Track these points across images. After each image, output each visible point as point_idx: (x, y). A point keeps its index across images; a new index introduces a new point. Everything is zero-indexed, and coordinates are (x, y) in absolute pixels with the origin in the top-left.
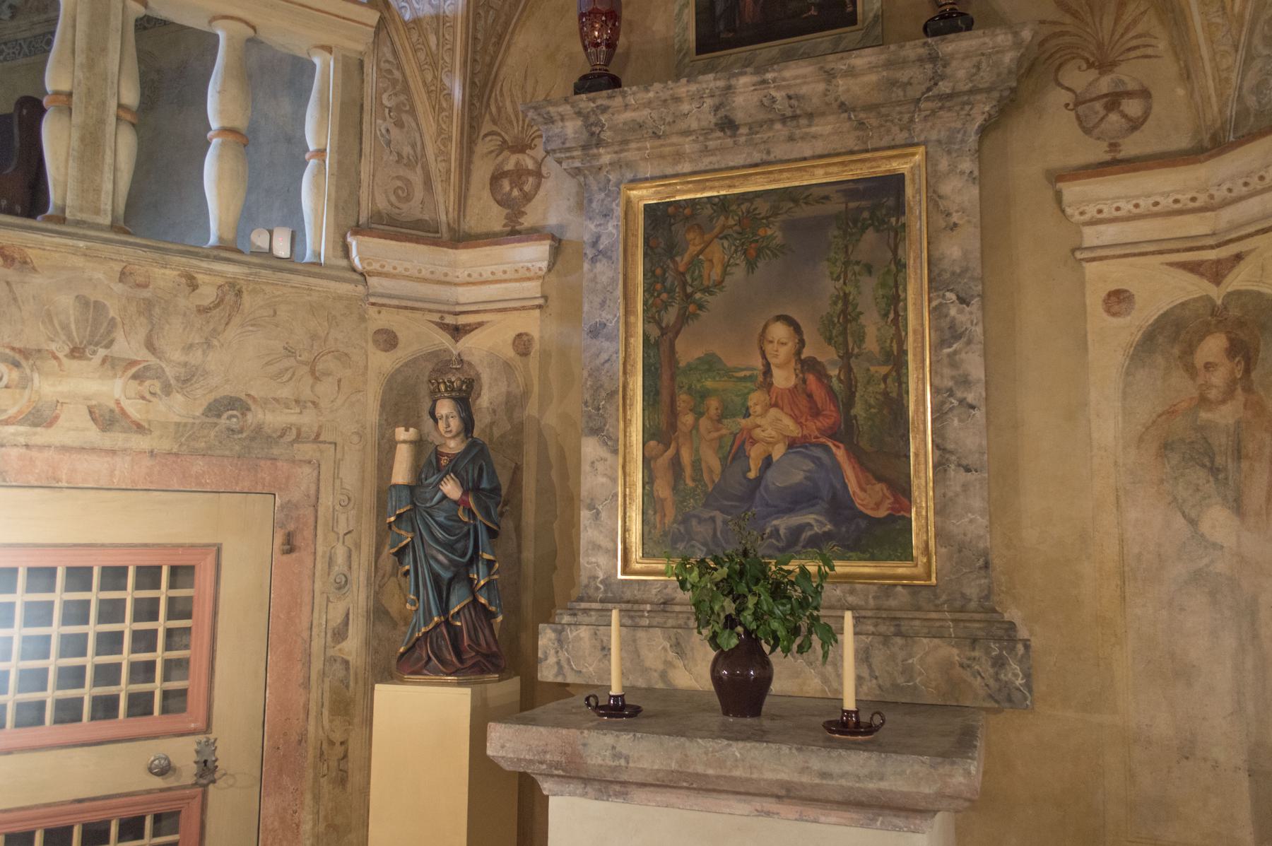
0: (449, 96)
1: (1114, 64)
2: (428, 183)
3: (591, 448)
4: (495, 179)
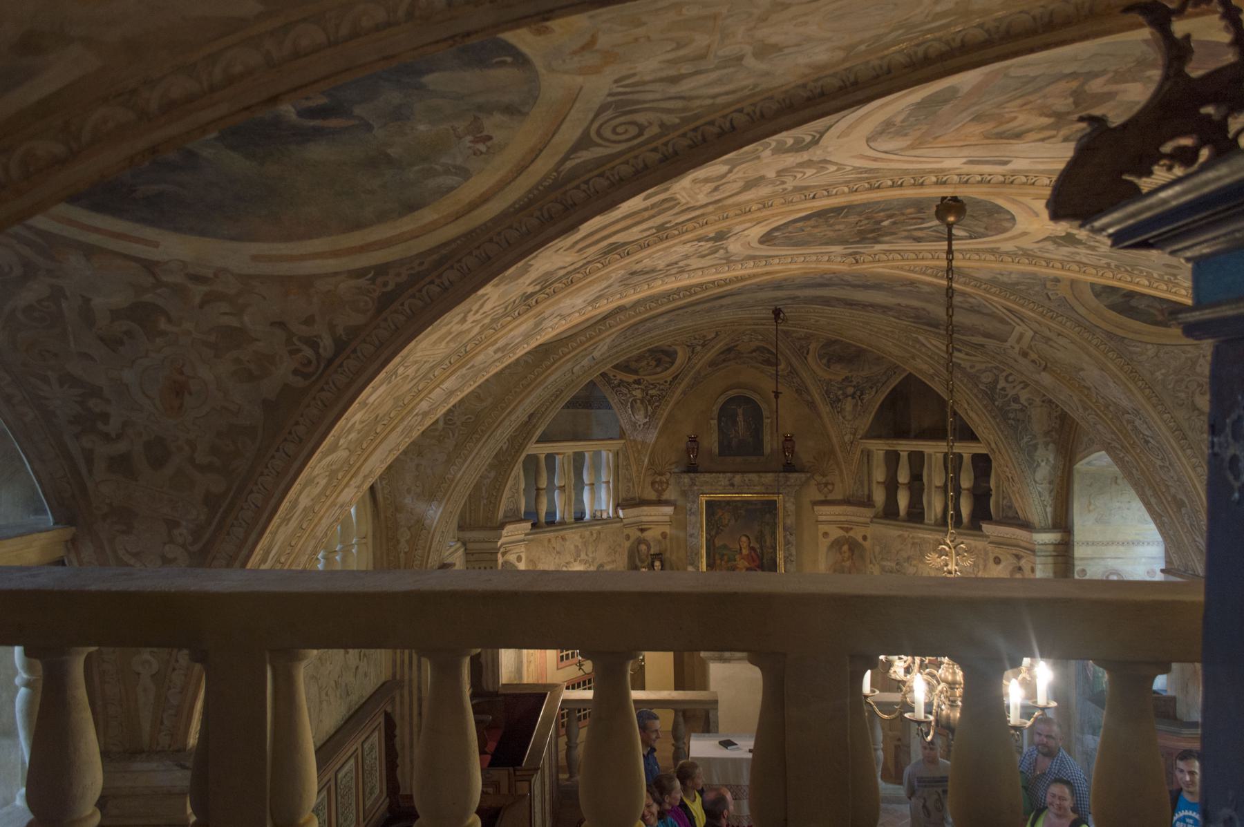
0: (643, 462)
1: (826, 476)
2: (634, 487)
4: (653, 483)
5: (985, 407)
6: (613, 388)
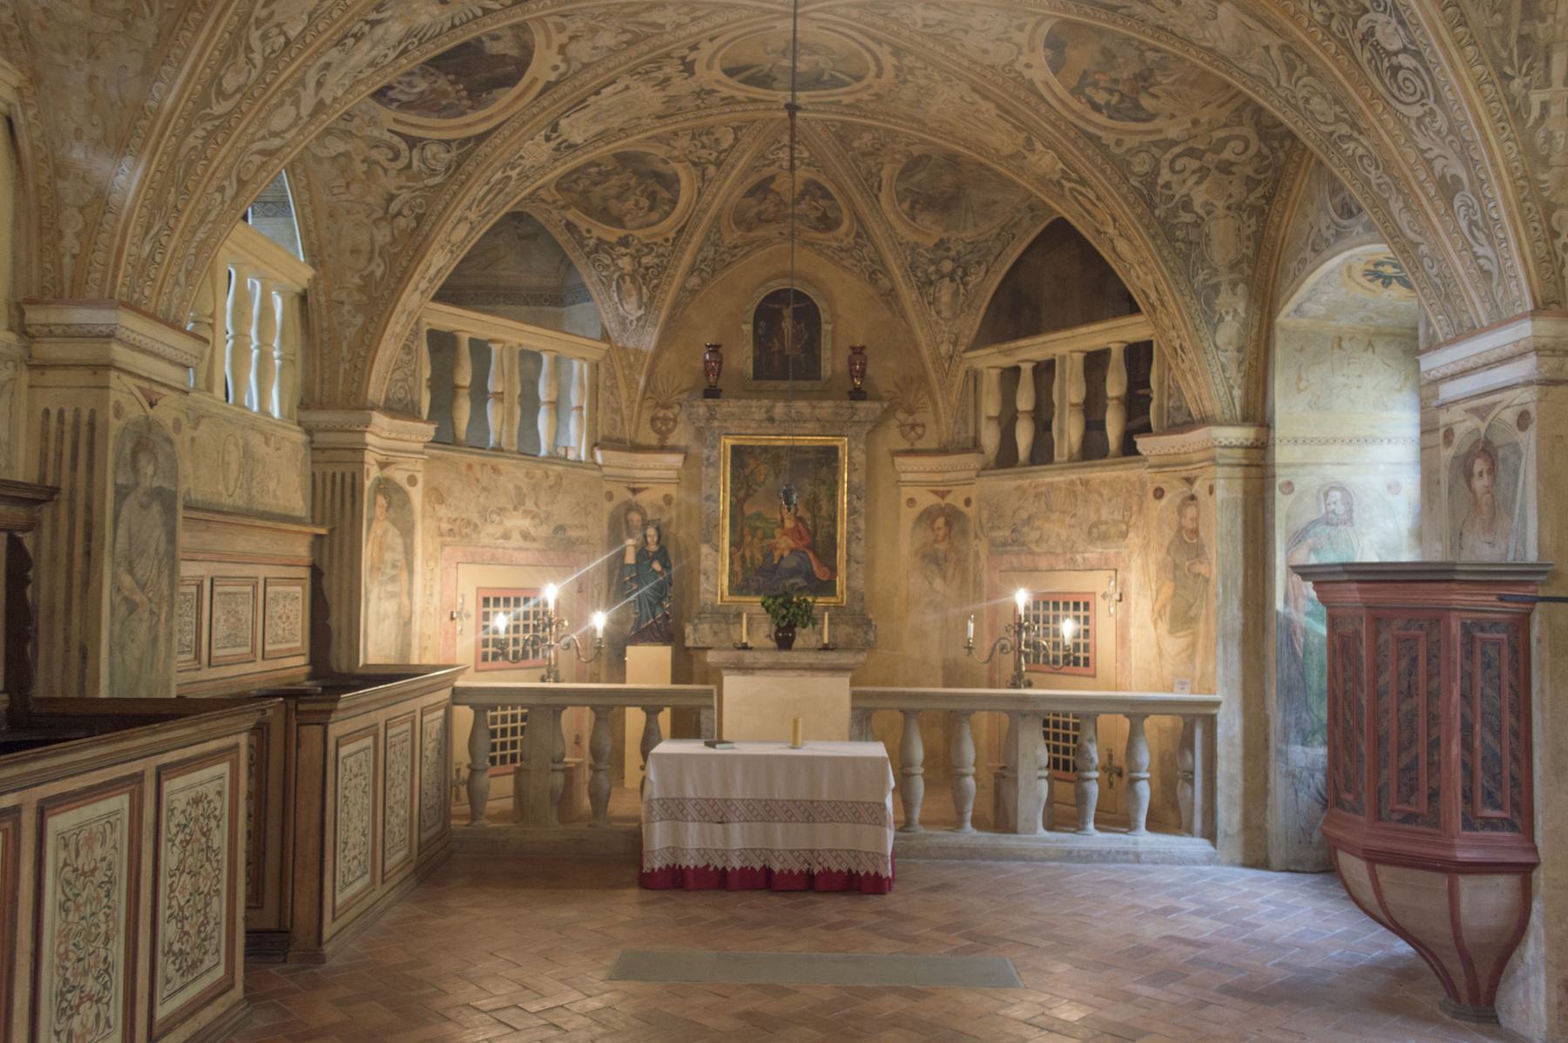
0: (638, 383)
3: (705, 549)
4: (653, 420)
5: (1140, 218)
6: (588, 255)
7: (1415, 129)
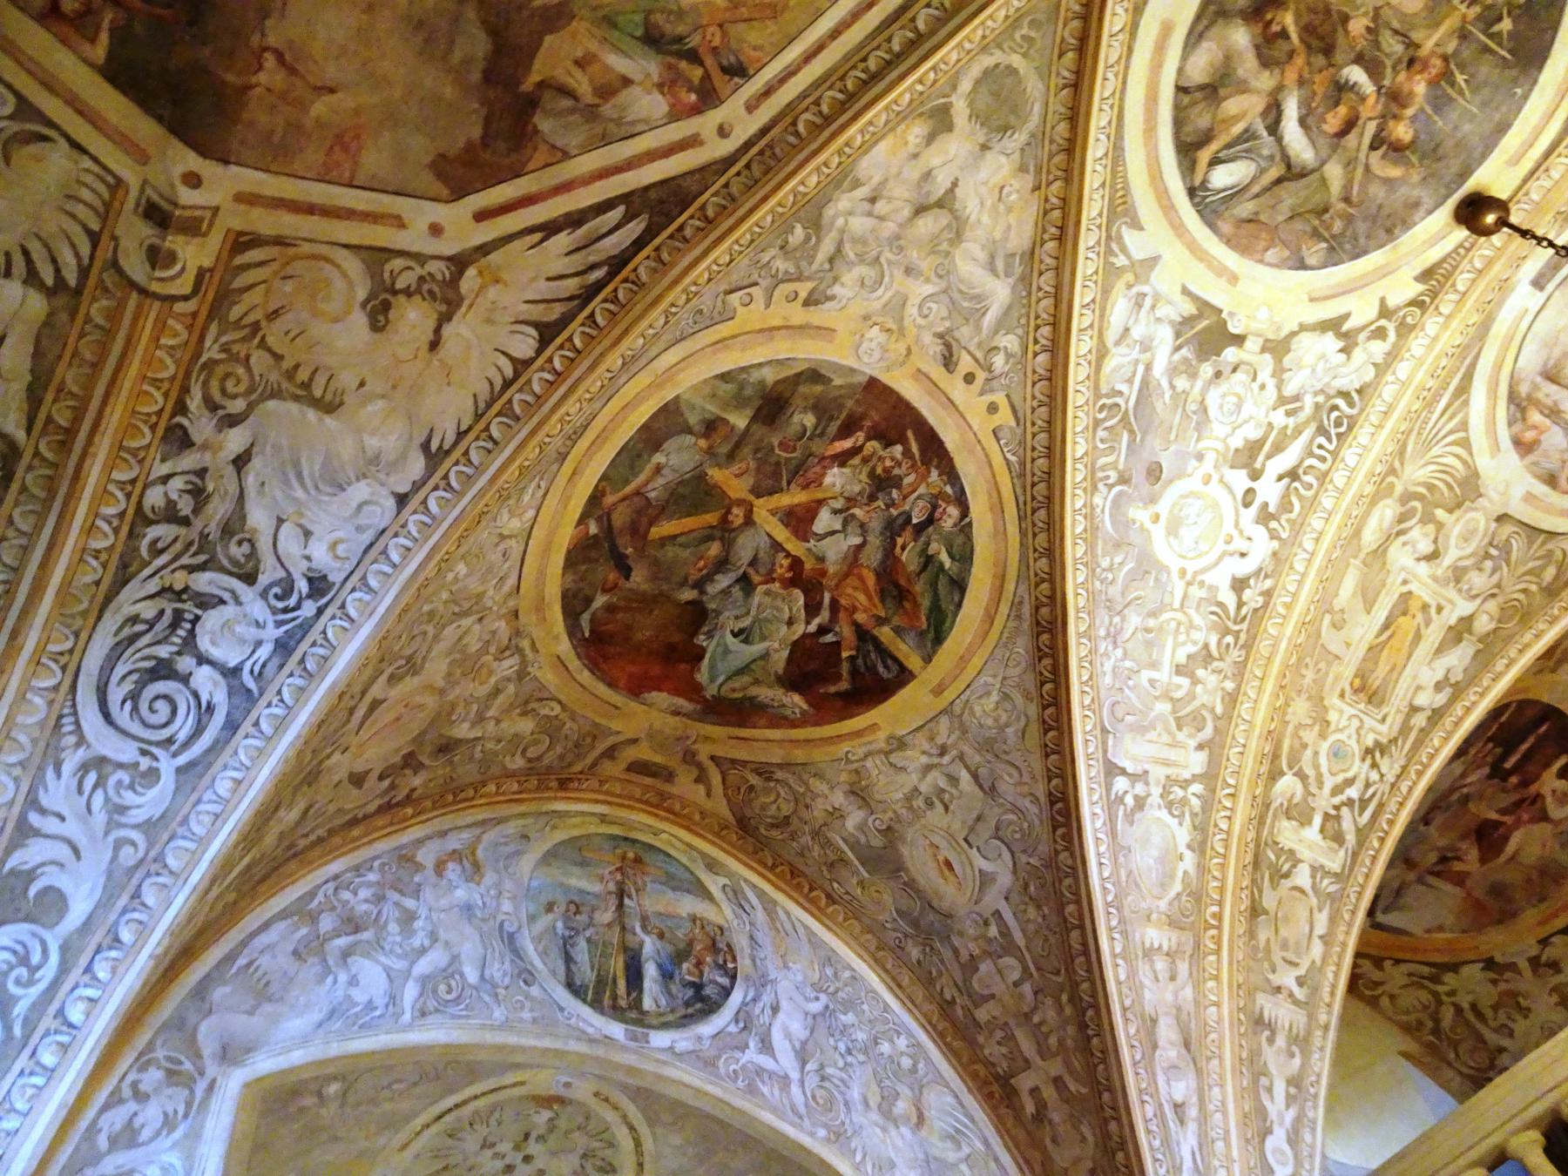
7: (67, 768)
